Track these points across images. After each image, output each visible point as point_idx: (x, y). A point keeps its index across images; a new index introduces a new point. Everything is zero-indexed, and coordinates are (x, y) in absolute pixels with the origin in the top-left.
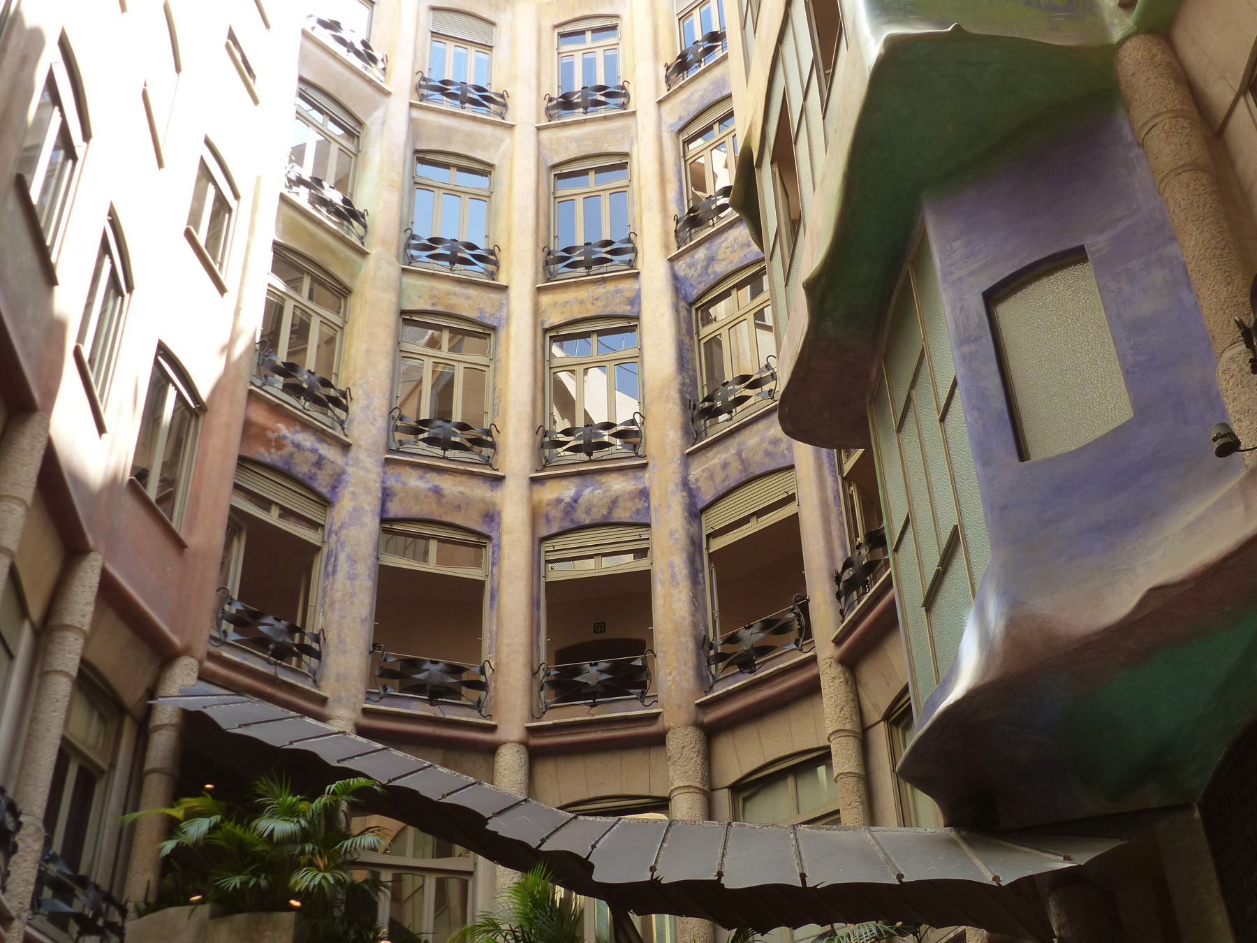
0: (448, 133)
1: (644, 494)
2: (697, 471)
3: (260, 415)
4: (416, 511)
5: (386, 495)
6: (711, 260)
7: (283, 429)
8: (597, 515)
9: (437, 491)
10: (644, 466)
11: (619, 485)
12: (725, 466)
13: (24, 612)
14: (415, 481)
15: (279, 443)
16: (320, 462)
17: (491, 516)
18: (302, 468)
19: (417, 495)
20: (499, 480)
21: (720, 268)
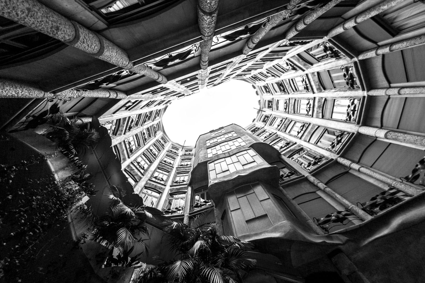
0: (152, 130)
1: (141, 178)
2: (149, 182)
3: (127, 119)
4: (119, 148)
5: (120, 143)
6: (164, 166)
7: (126, 123)
8: (133, 174)
9: (123, 151)
10: (143, 175)
11: (139, 173)
12: (153, 185)
13: (118, 85)
14: (124, 146)
15: (124, 123)
16: (122, 131)
17: (125, 160)
18: (120, 129)
19: (122, 148)
20: (129, 158)
21: (164, 168)
